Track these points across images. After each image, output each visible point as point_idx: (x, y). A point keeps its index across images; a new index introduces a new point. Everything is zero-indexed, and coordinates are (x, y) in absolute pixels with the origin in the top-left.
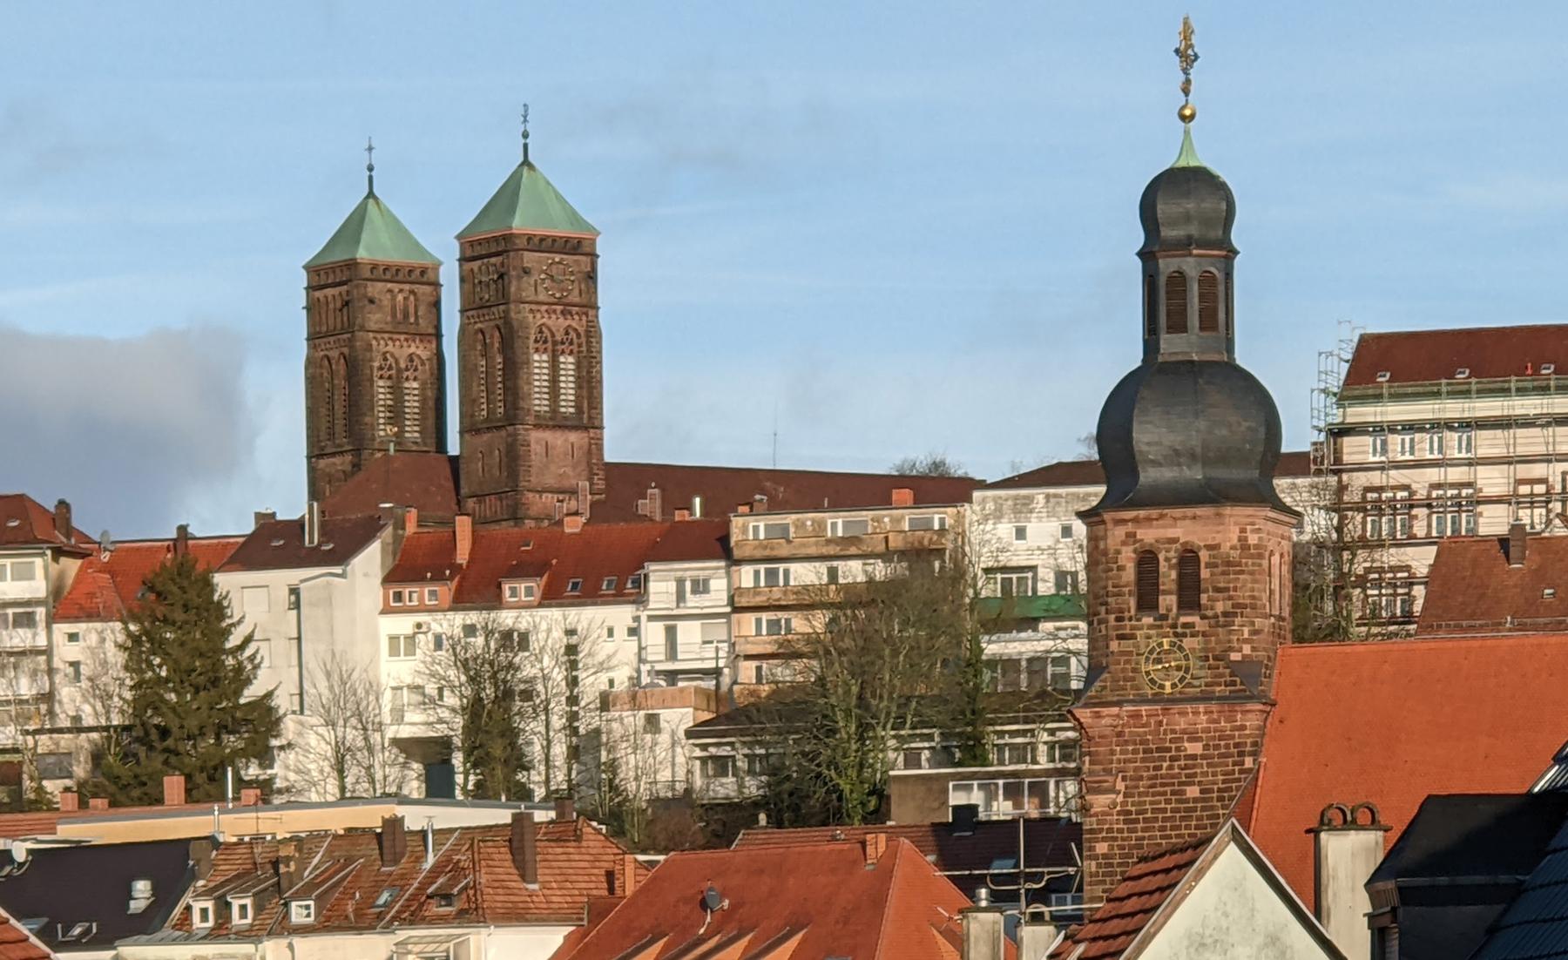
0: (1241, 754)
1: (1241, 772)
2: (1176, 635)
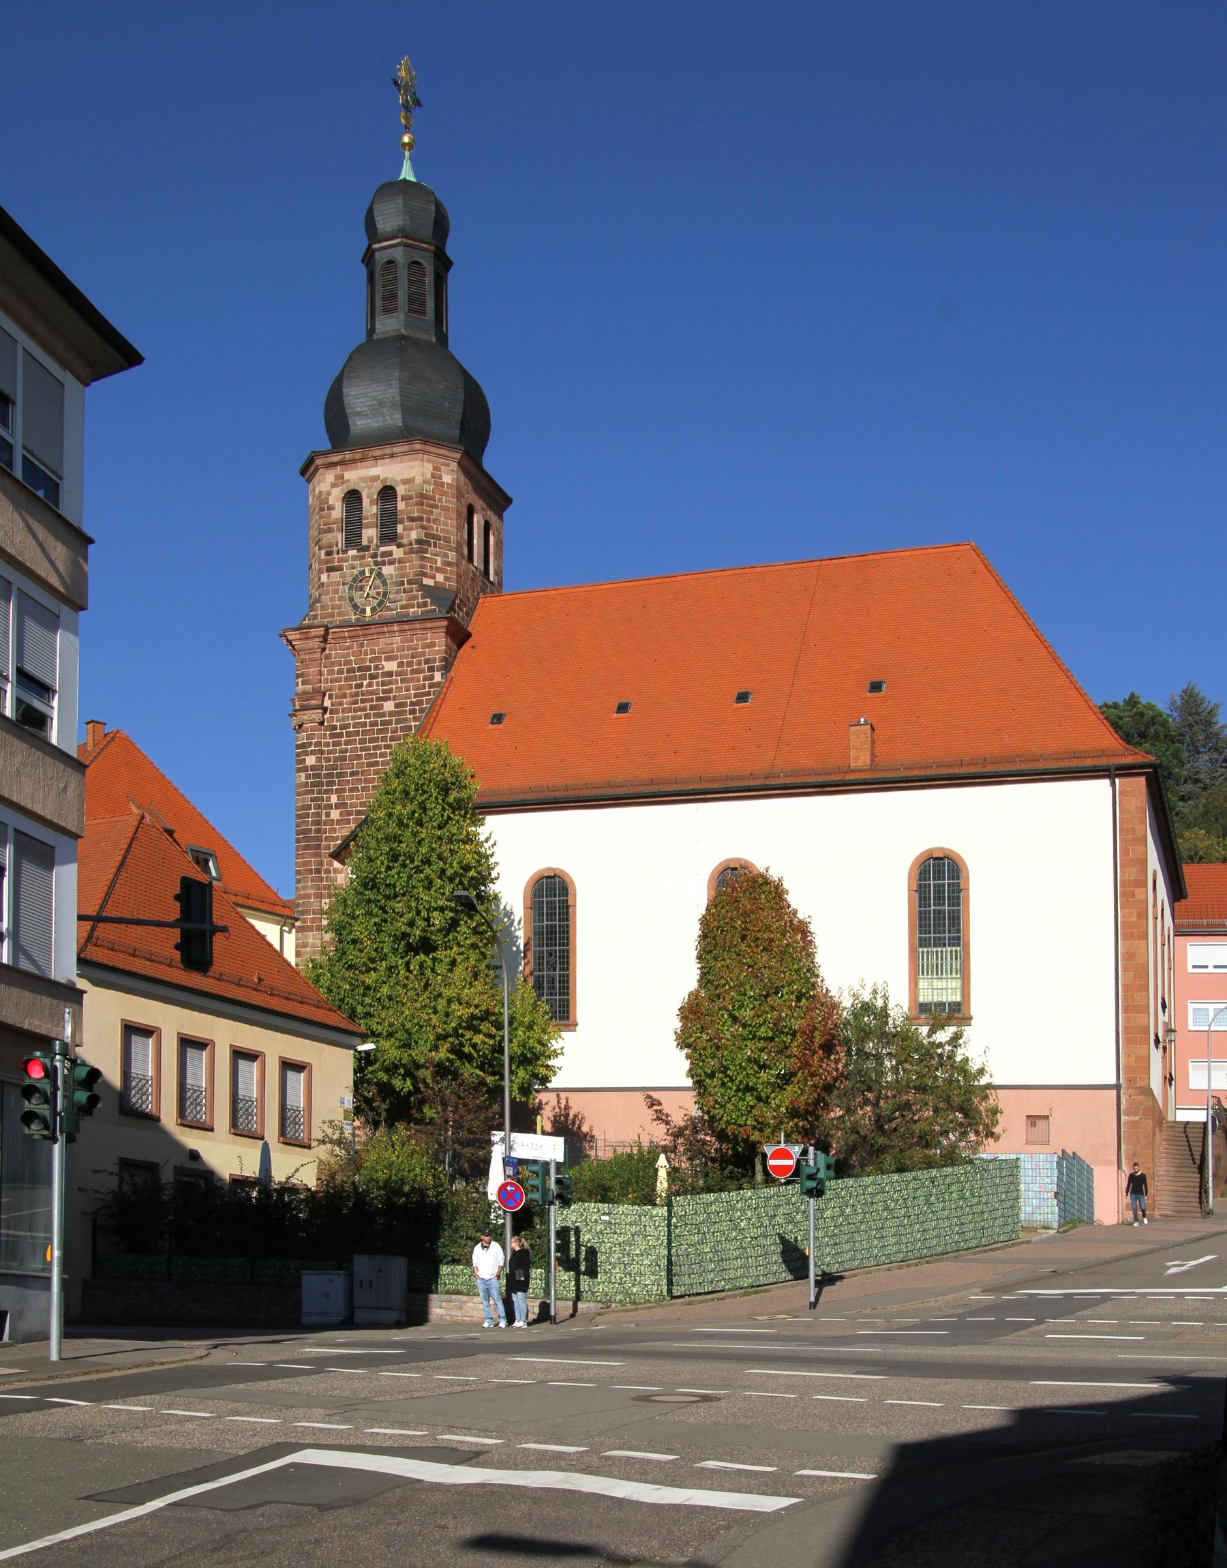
0: (431, 669)
1: (431, 686)
2: (376, 563)
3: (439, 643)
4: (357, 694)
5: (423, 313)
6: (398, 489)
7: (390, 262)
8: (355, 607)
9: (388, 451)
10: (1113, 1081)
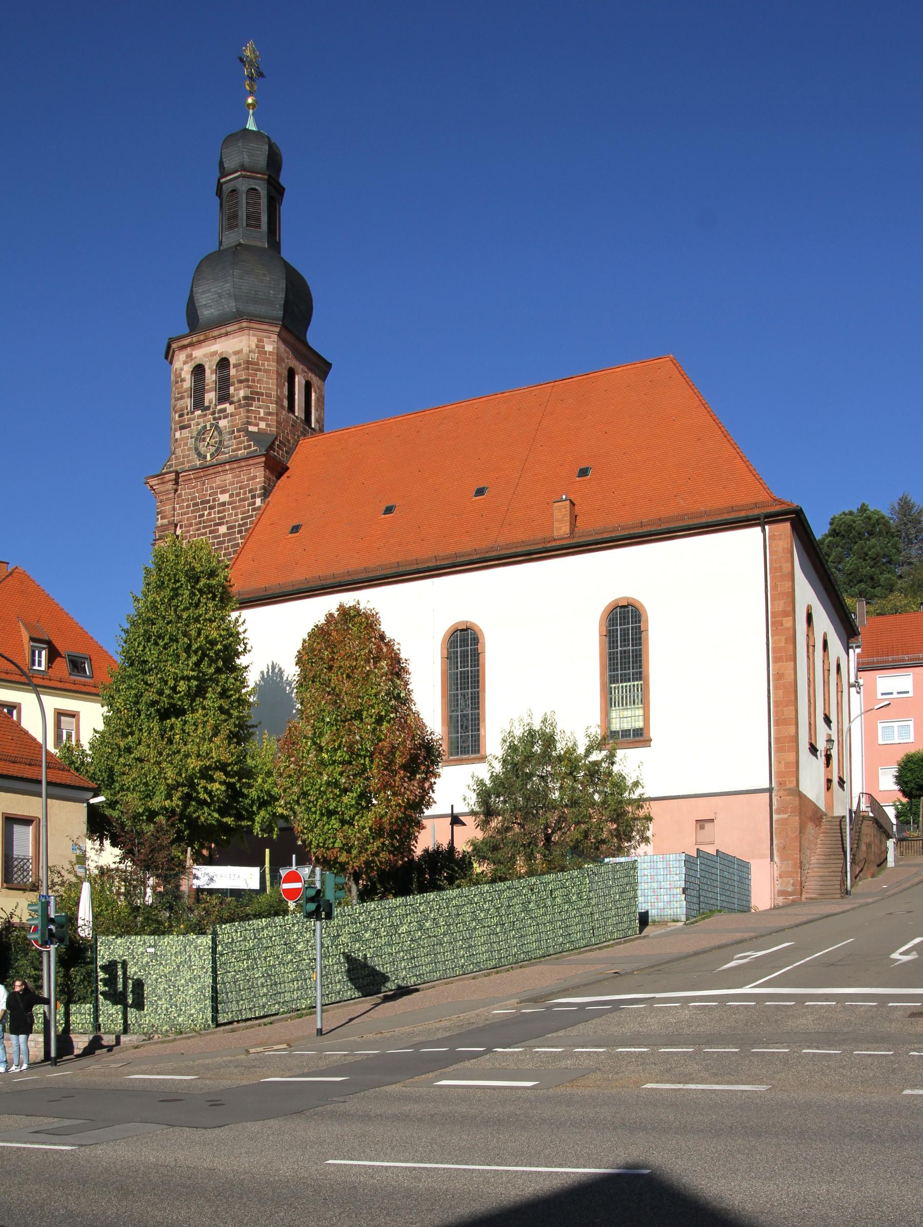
0: (254, 497)
1: (253, 510)
3: (259, 475)
4: (200, 523)
5: (259, 226)
6: (230, 360)
7: (233, 191)
8: (199, 454)
9: (223, 331)
10: (767, 785)
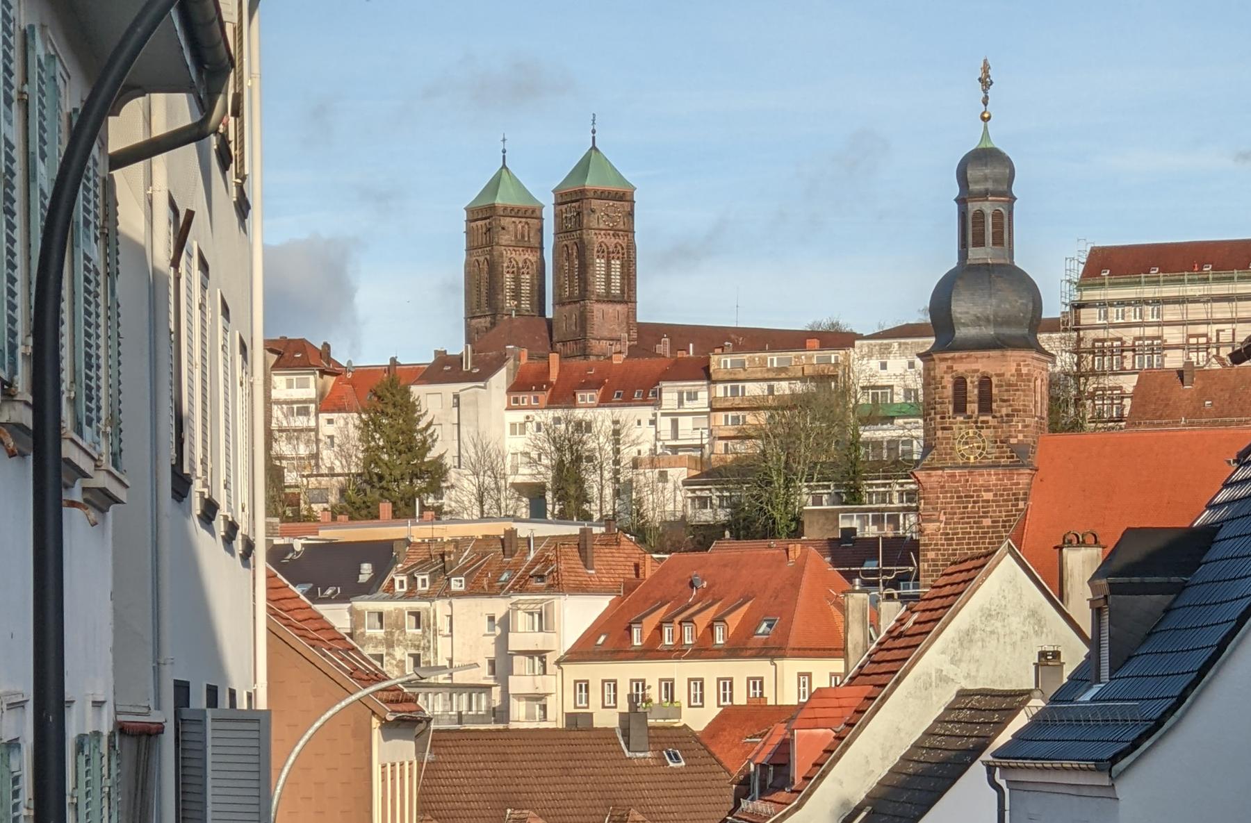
0: (1017, 500)
